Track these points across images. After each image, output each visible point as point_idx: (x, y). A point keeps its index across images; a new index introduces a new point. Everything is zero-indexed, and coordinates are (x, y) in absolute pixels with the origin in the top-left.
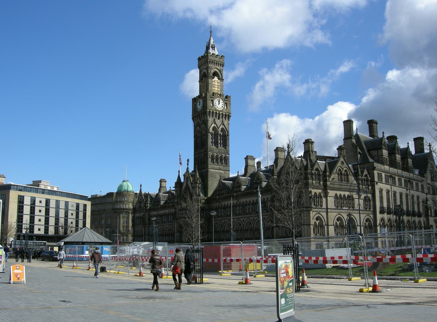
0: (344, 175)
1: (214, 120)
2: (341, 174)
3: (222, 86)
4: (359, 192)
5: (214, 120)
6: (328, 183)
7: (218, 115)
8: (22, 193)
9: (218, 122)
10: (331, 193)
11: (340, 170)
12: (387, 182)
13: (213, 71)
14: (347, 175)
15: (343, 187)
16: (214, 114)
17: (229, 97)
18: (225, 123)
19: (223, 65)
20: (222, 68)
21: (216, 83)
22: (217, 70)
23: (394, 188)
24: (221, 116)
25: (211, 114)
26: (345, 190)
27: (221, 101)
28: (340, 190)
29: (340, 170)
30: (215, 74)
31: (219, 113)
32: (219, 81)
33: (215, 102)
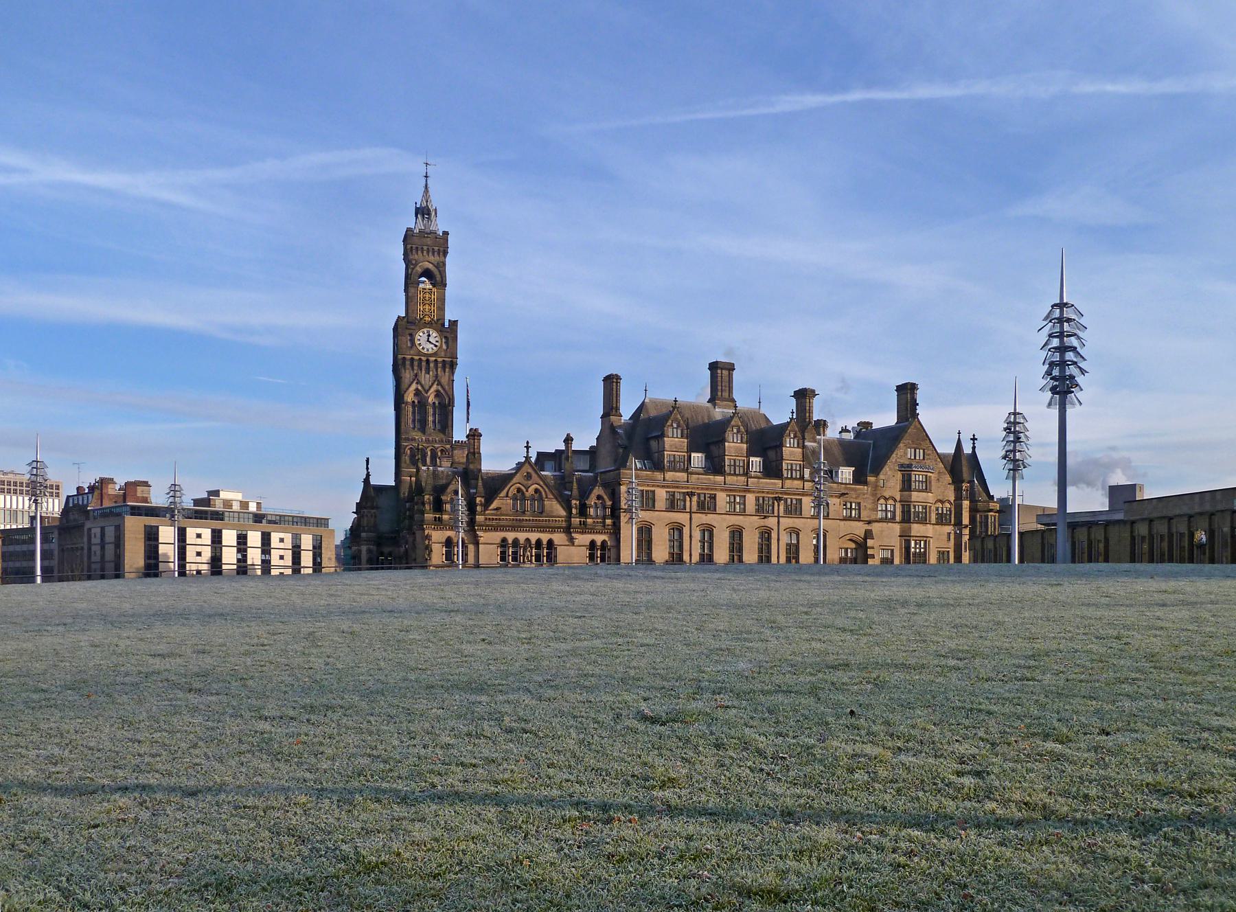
0: (533, 499)
1: (416, 375)
2: (524, 498)
3: (442, 300)
4: (568, 530)
5: (416, 375)
6: (480, 518)
7: (424, 364)
8: (152, 521)
9: (426, 379)
10: (484, 536)
11: (519, 490)
12: (672, 506)
13: (419, 269)
14: (541, 500)
15: (524, 523)
16: (416, 363)
17: (454, 324)
18: (444, 380)
19: (445, 253)
20: (442, 259)
21: (427, 296)
22: (431, 266)
23: (700, 518)
24: (432, 365)
25: (408, 363)
26: (532, 529)
27: (434, 334)
28: (514, 528)
29: (519, 490)
30: (427, 273)
31: (428, 361)
32: (435, 290)
33: (417, 337)
